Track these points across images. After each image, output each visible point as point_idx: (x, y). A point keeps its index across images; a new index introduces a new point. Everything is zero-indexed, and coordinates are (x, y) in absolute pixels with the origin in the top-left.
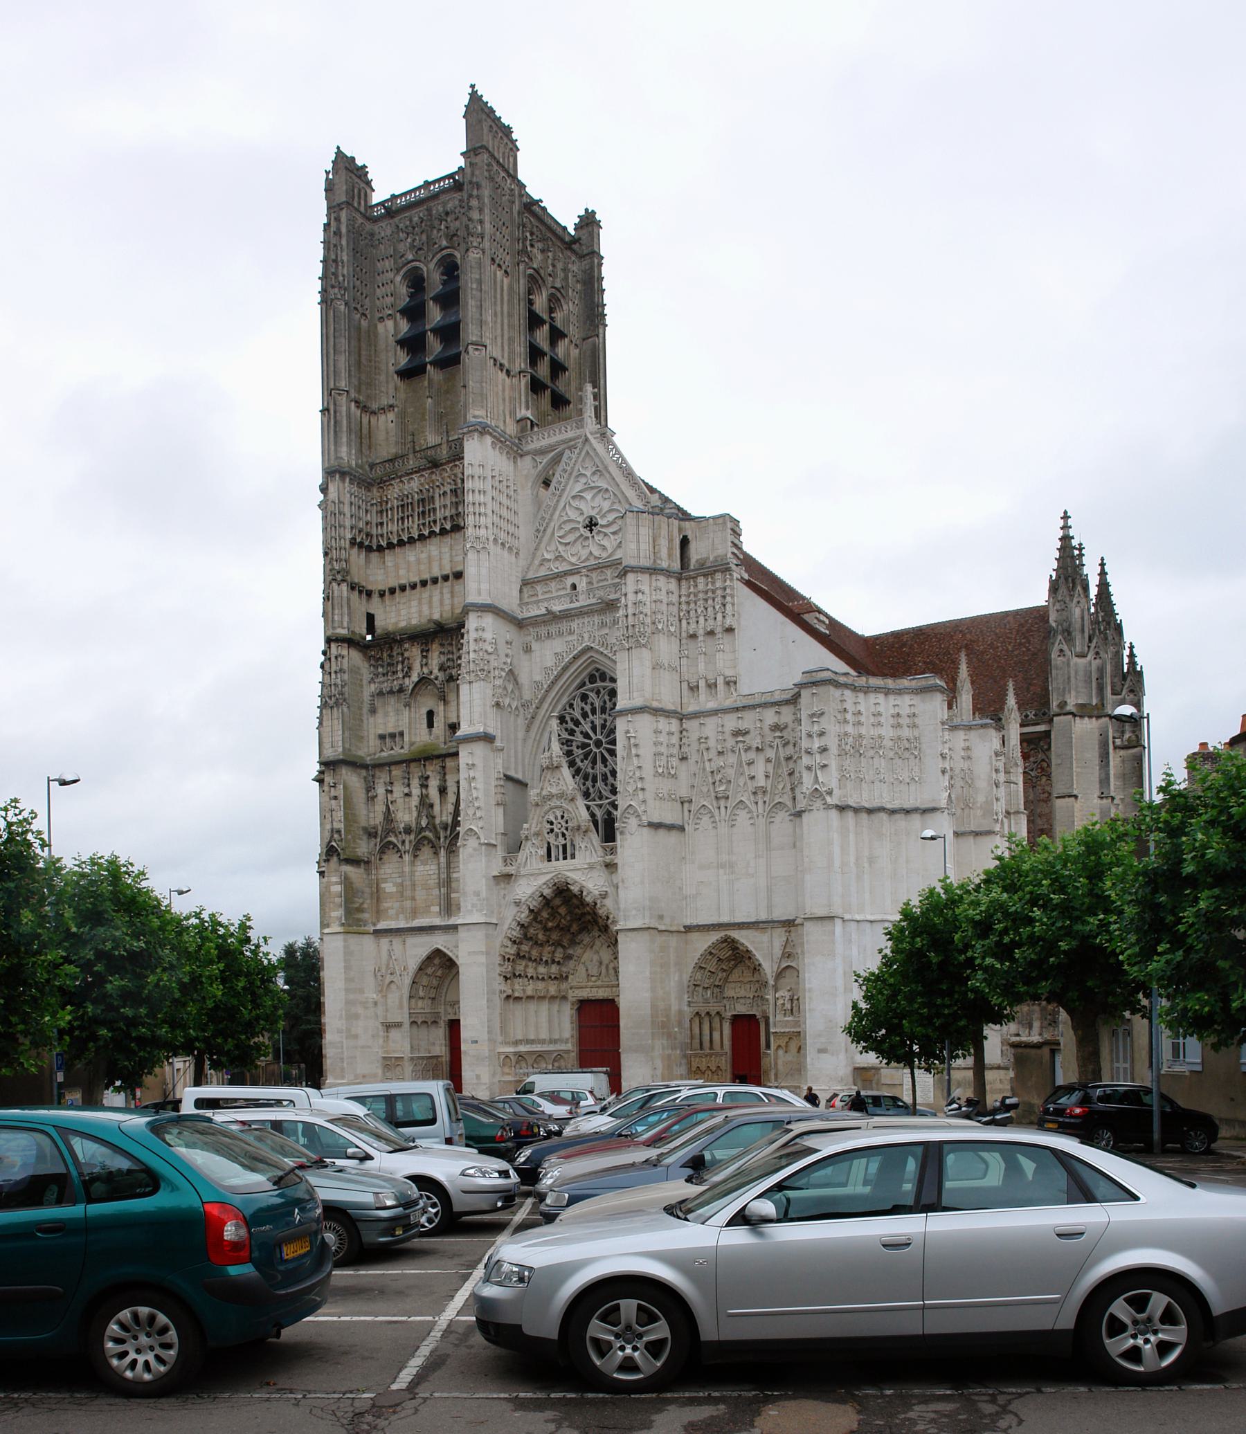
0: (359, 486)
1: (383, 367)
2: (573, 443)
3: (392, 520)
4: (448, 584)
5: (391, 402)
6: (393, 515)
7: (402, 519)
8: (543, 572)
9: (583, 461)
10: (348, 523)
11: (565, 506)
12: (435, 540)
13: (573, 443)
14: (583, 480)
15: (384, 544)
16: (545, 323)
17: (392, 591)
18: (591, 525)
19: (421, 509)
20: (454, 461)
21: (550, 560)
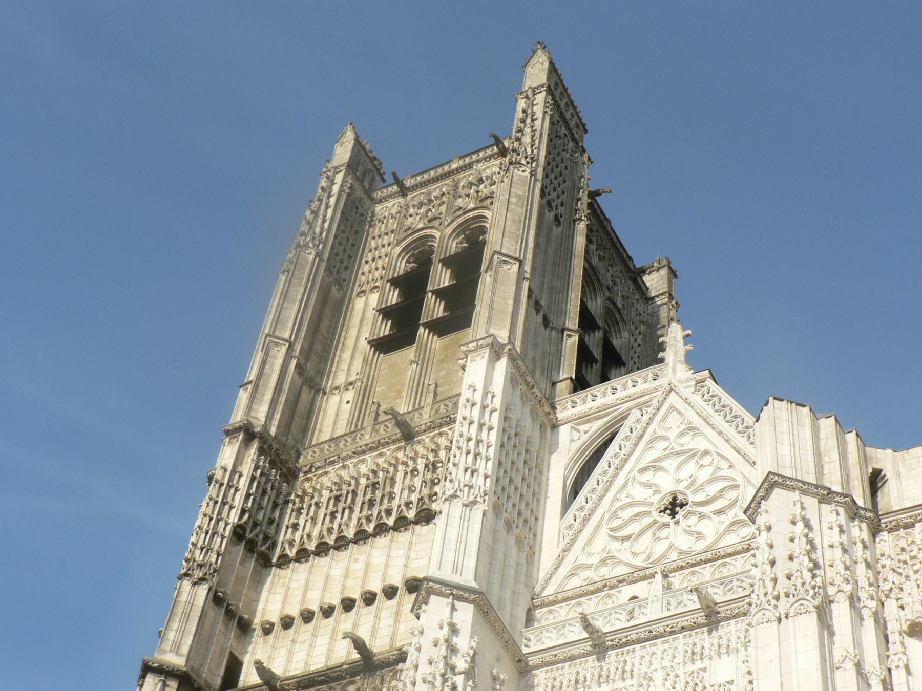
0: (273, 464)
1: (350, 343)
2: (646, 398)
3: (314, 519)
4: (394, 602)
5: (353, 378)
6: (316, 513)
7: (333, 515)
8: (575, 582)
9: (664, 419)
10: (238, 500)
11: (625, 485)
12: (382, 541)
13: (646, 398)
14: (663, 445)
15: (292, 553)
16: (599, 328)
17: (287, 623)
18: (674, 506)
19: (368, 497)
20: (441, 426)
21: (589, 567)
